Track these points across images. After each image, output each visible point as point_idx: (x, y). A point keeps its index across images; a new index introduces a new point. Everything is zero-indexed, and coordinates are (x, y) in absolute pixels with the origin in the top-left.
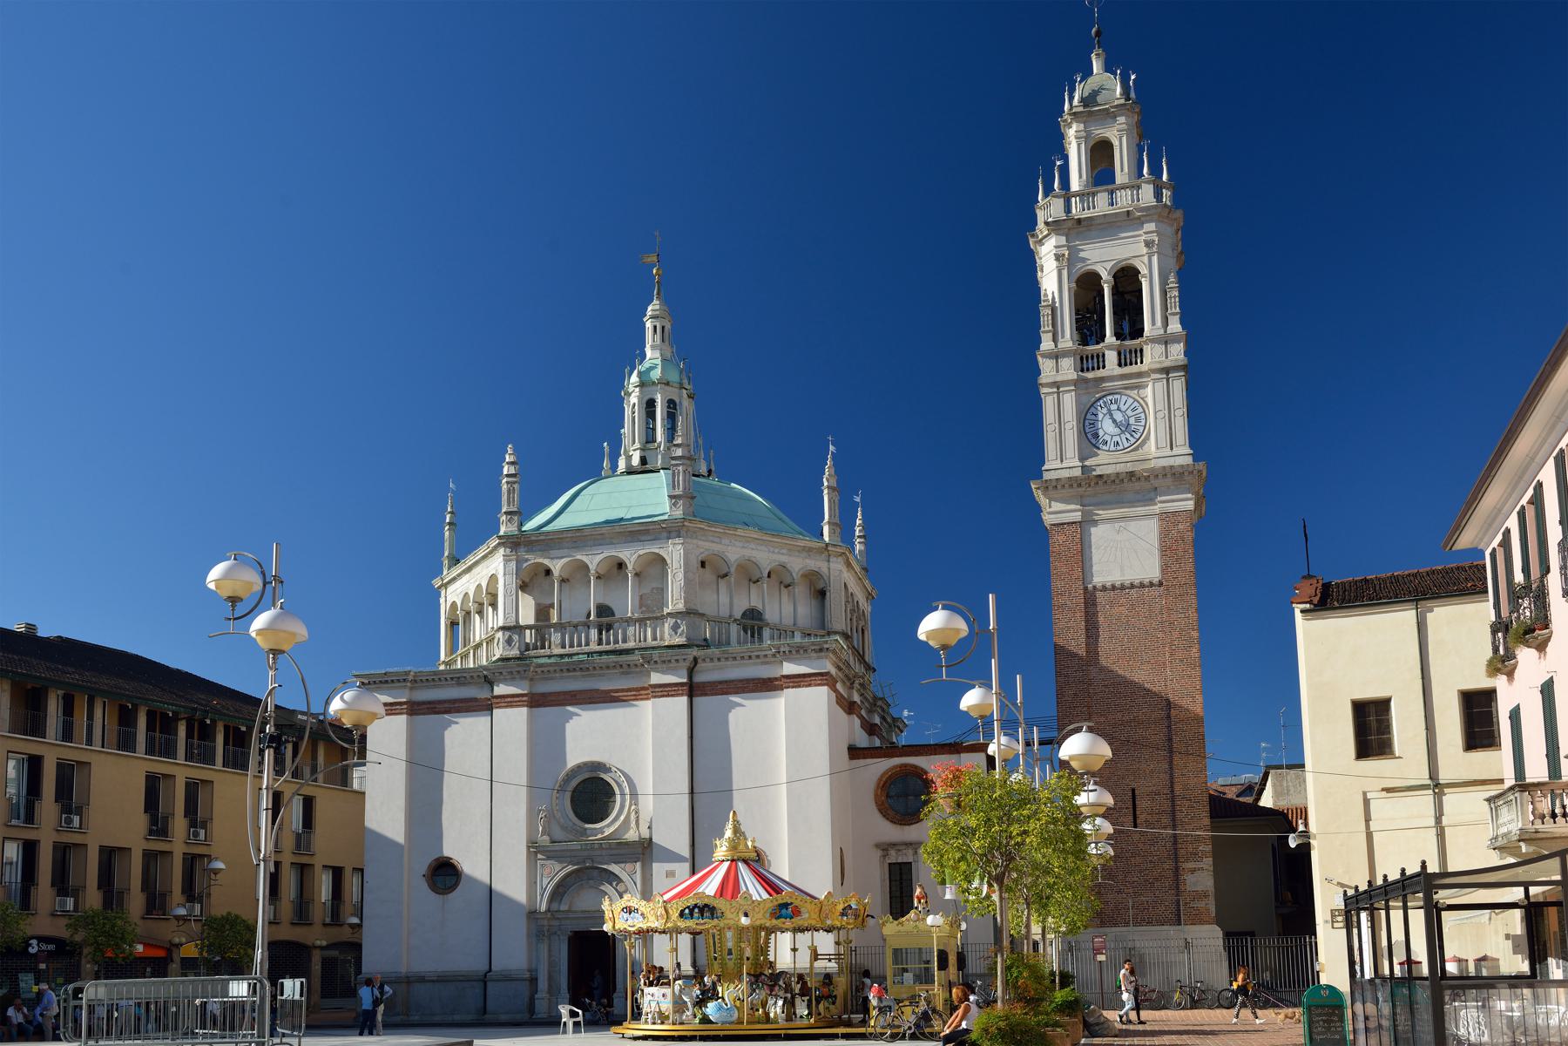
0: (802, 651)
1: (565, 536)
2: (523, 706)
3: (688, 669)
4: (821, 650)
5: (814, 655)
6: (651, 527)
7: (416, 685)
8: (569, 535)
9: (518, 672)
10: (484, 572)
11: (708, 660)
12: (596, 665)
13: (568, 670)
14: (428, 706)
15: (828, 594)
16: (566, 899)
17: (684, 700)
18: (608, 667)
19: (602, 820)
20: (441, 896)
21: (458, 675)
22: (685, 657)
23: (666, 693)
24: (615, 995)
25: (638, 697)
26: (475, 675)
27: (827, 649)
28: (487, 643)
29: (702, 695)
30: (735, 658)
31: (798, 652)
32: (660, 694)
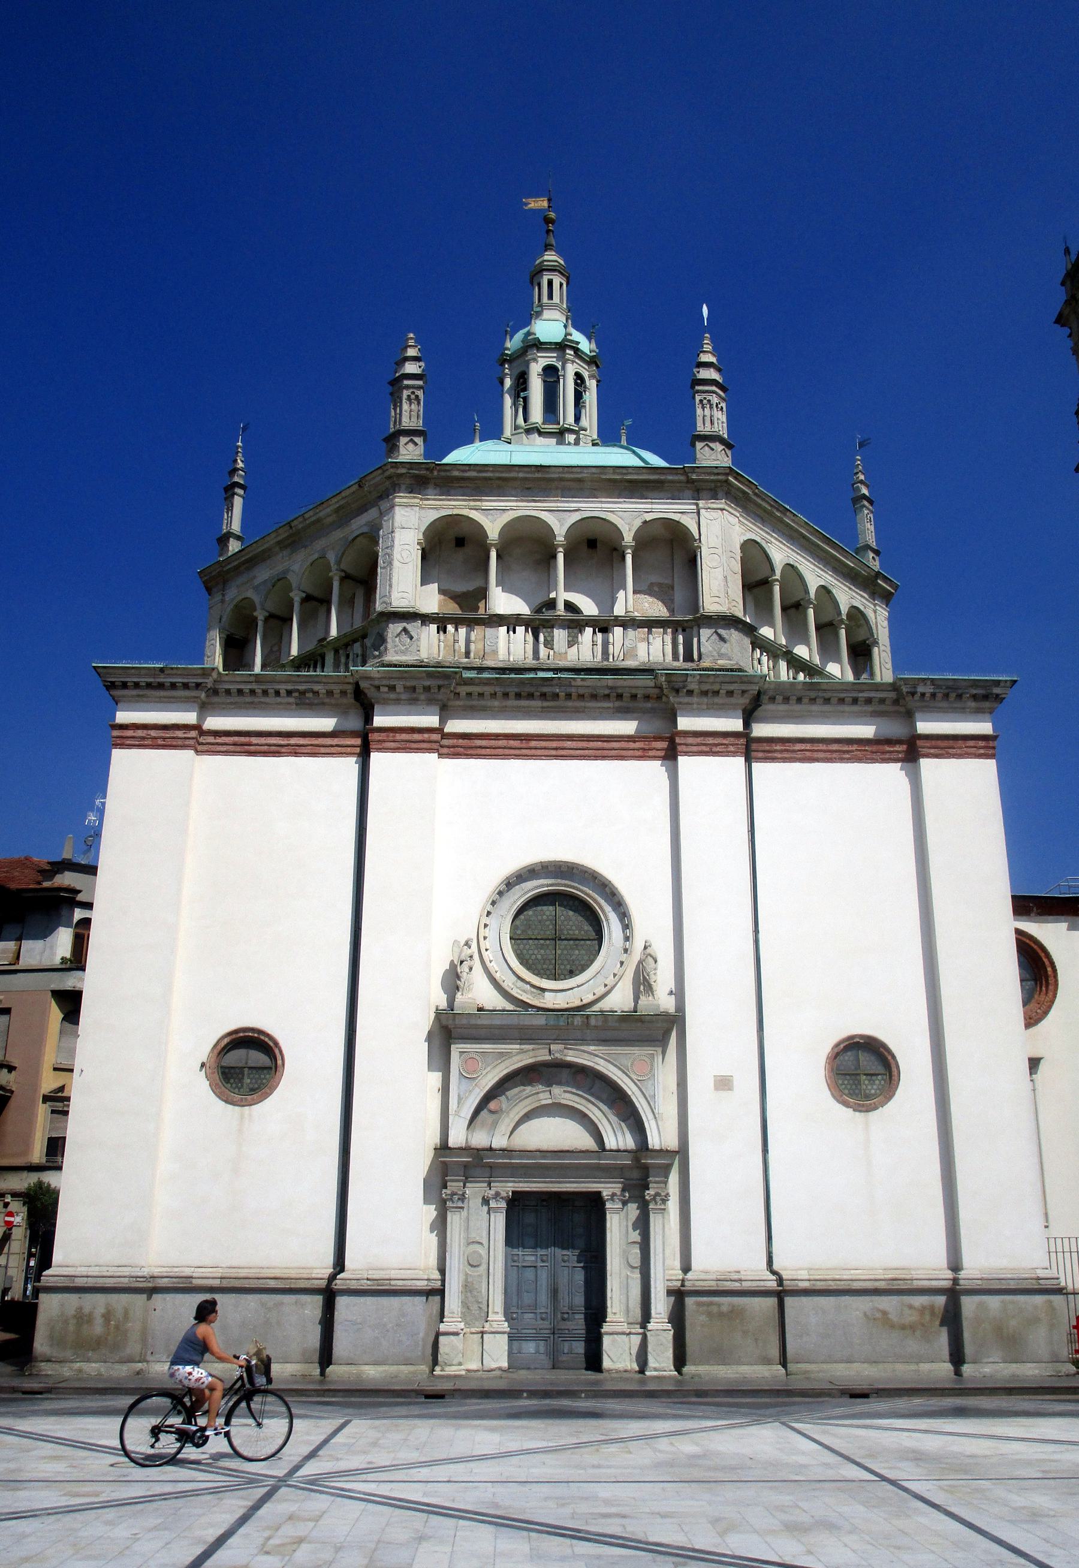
0: (953, 695)
1: (513, 475)
2: (429, 750)
3: (744, 711)
4: (986, 697)
5: (972, 704)
6: (670, 477)
7: (216, 699)
8: (521, 475)
9: (427, 689)
10: (338, 534)
11: (779, 698)
12: (573, 690)
13: (518, 696)
14: (236, 739)
15: (876, 650)
16: (506, 1124)
17: (741, 760)
18: (594, 697)
19: (572, 974)
20: (237, 1108)
21: (302, 687)
22: (744, 687)
23: (704, 748)
24: (606, 1328)
25: (651, 753)
26: (337, 689)
27: (997, 695)
28: (336, 651)
29: (765, 759)
30: (827, 701)
31: (946, 696)
32: (695, 749)
